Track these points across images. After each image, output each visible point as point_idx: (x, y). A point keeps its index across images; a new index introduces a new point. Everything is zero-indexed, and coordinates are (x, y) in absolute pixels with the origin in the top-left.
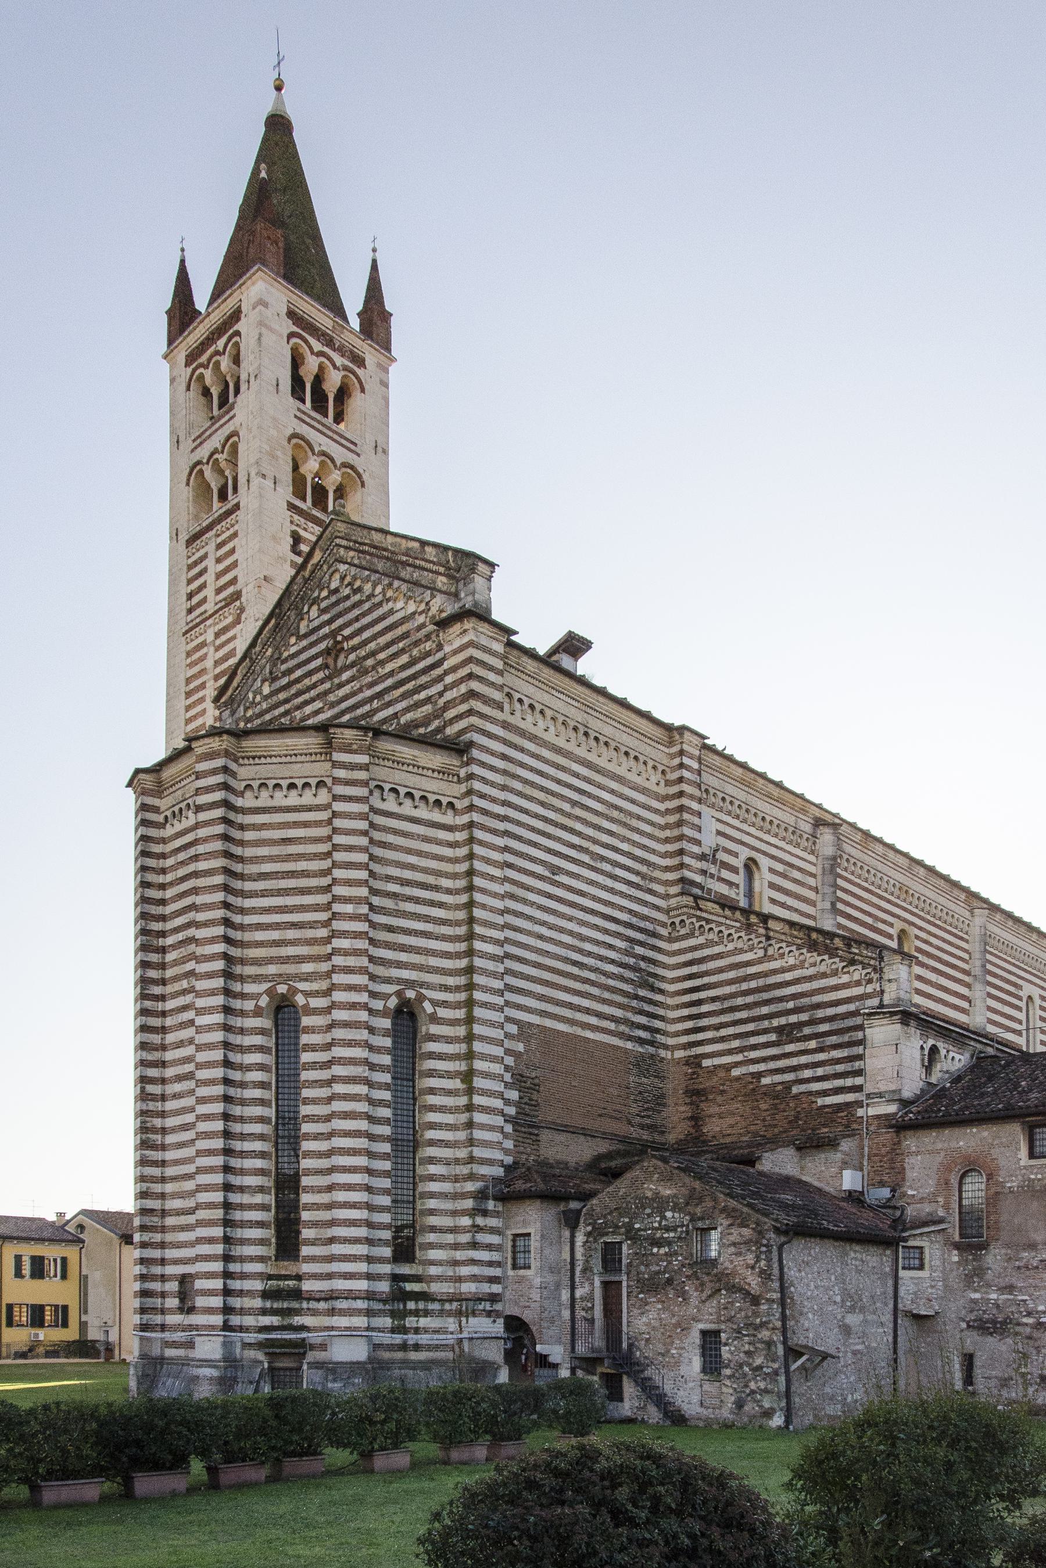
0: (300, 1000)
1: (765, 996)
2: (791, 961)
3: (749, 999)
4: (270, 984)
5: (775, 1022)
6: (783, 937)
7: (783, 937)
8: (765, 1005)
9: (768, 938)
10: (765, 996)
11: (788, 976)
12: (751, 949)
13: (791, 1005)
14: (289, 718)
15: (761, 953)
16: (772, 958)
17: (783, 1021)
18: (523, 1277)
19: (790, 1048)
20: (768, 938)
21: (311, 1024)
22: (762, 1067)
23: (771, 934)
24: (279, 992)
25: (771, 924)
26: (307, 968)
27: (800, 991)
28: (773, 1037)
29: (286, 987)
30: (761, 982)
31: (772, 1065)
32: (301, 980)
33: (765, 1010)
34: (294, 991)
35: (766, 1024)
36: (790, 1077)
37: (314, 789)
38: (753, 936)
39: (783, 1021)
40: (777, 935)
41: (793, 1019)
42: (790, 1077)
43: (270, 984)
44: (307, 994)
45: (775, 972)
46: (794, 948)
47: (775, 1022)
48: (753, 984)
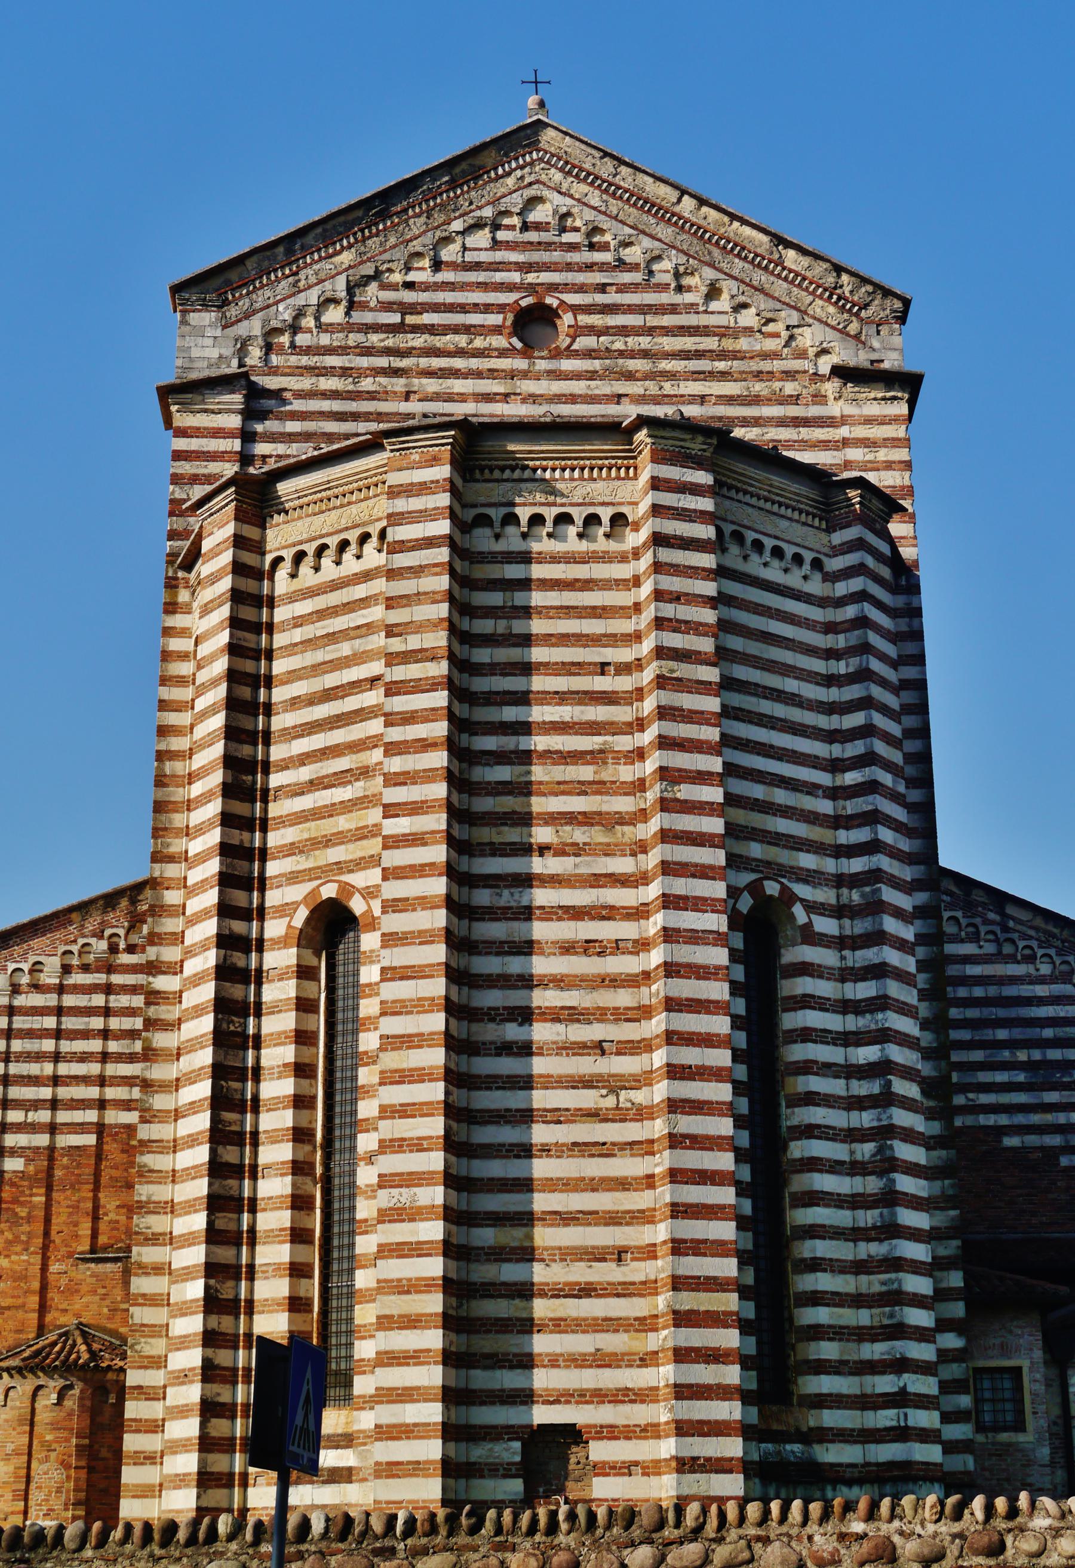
0: (800, 914)
1: (1002, 1013)
2: (1045, 969)
3: (972, 1013)
4: (753, 876)
5: (1022, 1056)
6: (1032, 933)
7: (1032, 933)
8: (1003, 1027)
9: (1006, 929)
10: (1002, 1013)
11: (1041, 990)
12: (975, 938)
13: (1048, 1033)
14: (402, 381)
15: (990, 948)
16: (1012, 959)
17: (1037, 1055)
18: (1009, 1445)
19: (1052, 1097)
20: (1006, 929)
21: (817, 961)
22: (1003, 1120)
23: (1011, 924)
24: (769, 892)
25: (1010, 910)
26: (807, 861)
27: (1062, 1014)
28: (1021, 1077)
29: (778, 886)
30: (992, 991)
31: (1020, 1119)
32: (799, 880)
33: (1002, 1034)
34: (788, 898)
35: (1006, 1054)
36: (1055, 1140)
37: (497, 524)
38: (978, 921)
39: (1037, 1055)
40: (1019, 927)
41: (1055, 1054)
42: (1055, 1140)
43: (753, 876)
44: (811, 907)
45: (1014, 980)
46: (1052, 952)
47: (1022, 1056)
48: (978, 992)
